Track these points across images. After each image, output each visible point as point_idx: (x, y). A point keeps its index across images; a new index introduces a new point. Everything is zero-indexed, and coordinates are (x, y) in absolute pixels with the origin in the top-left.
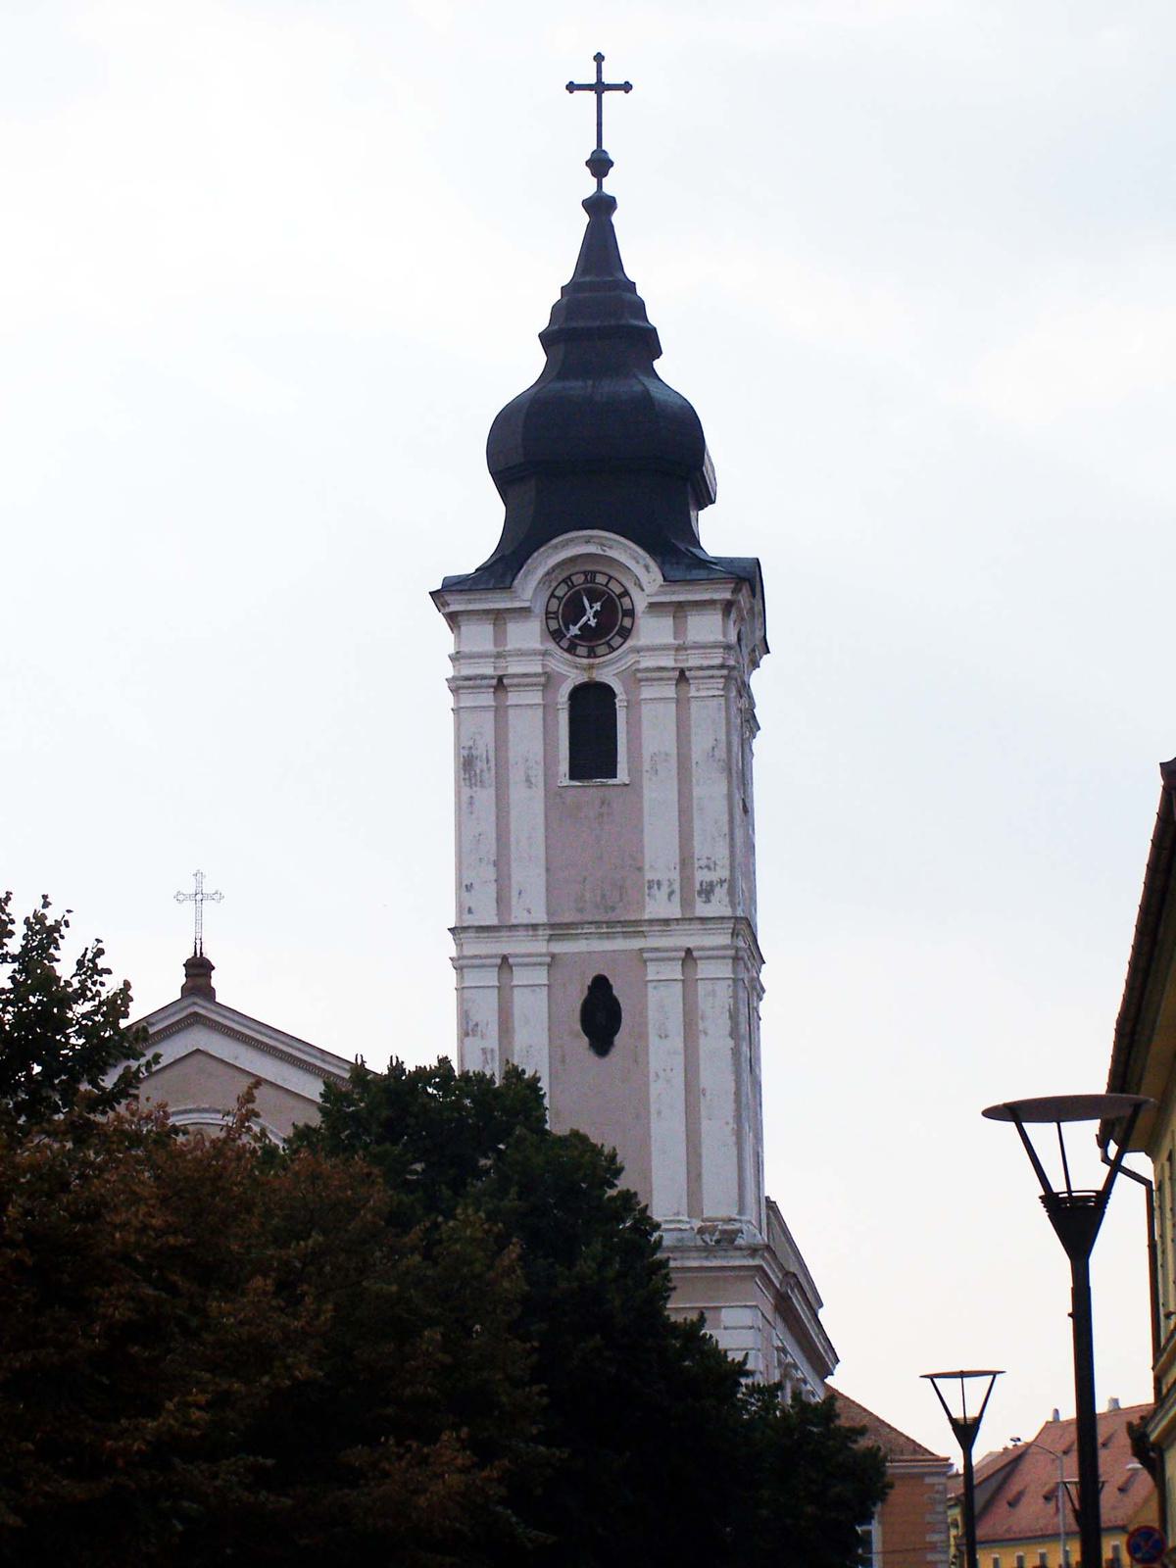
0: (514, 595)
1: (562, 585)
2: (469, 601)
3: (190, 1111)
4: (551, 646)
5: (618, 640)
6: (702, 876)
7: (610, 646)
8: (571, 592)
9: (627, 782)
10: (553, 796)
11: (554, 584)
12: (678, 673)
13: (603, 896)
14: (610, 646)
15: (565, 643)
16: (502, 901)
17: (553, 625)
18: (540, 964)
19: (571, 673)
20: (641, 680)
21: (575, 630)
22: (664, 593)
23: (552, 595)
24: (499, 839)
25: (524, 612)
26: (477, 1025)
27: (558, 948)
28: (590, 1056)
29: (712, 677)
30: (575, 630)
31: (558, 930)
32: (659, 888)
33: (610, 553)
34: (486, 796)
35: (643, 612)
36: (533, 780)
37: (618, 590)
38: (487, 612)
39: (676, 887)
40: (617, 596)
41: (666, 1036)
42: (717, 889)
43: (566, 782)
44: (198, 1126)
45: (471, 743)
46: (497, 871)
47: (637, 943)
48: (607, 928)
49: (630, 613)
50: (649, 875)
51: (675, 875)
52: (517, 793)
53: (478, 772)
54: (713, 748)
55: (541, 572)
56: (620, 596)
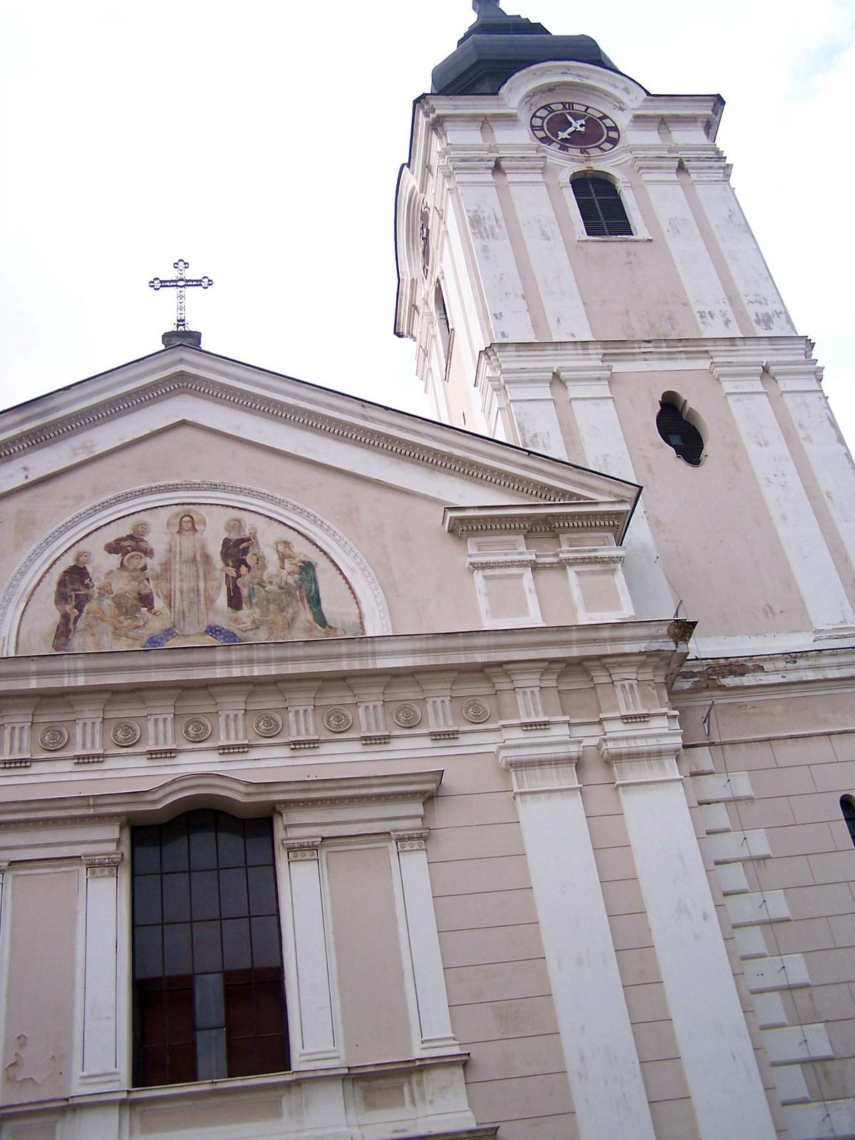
0: (501, 103)
1: (542, 110)
2: (456, 107)
3: (175, 488)
5: (607, 146)
8: (551, 115)
9: (651, 238)
10: (573, 249)
12: (677, 163)
13: (652, 326)
14: (601, 149)
16: (538, 320)
17: (541, 134)
18: (599, 379)
20: (640, 168)
21: (563, 135)
22: (647, 108)
23: (534, 116)
24: (523, 278)
25: (510, 119)
26: (535, 436)
28: (682, 464)
29: (710, 168)
31: (614, 348)
32: (712, 317)
34: (502, 248)
35: (628, 126)
36: (550, 234)
38: (474, 118)
39: (731, 316)
40: (598, 118)
41: (766, 445)
42: (775, 319)
44: (186, 507)
45: (476, 208)
46: (527, 304)
49: (615, 129)
50: (696, 309)
51: (727, 307)
52: (534, 246)
53: (488, 227)
54: (730, 217)
55: (524, 91)
56: (601, 118)
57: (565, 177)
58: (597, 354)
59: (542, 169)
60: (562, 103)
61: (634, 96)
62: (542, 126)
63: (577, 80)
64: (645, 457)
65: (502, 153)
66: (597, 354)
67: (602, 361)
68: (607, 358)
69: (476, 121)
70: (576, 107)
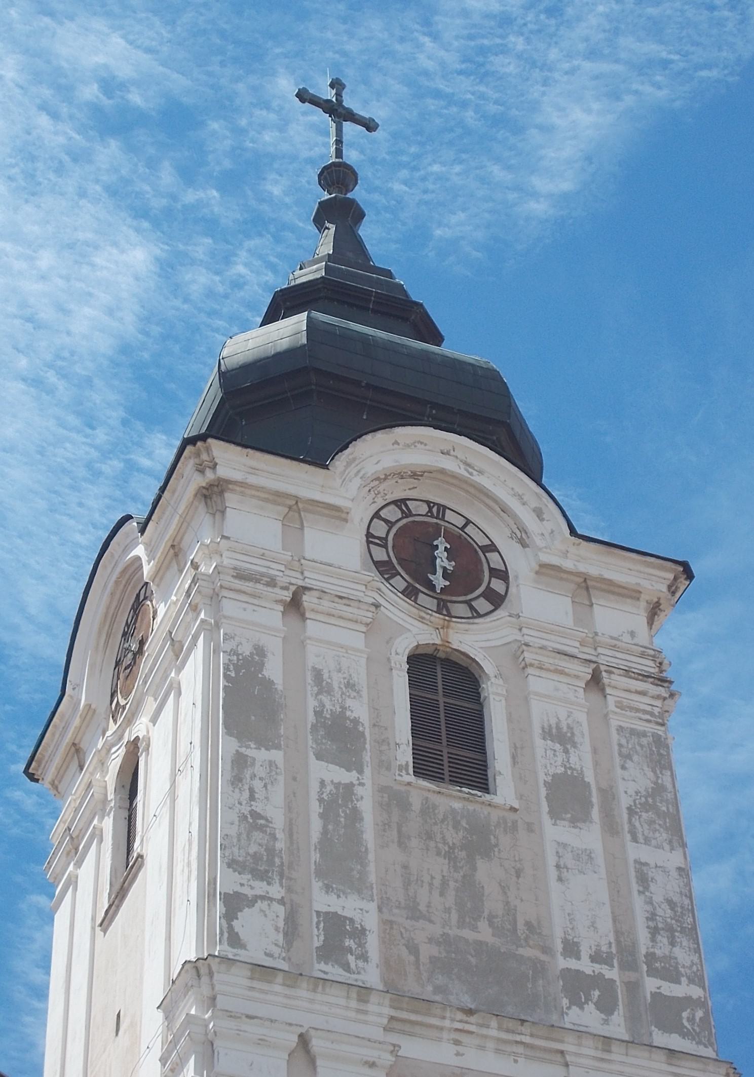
5: (482, 605)
7: (472, 608)
8: (405, 521)
11: (380, 502)
14: (472, 608)
17: (380, 554)
23: (377, 515)
33: (477, 478)
38: (277, 497)
48: (500, 1028)
49: (503, 575)
57: (403, 647)
58: (380, 1015)
59: (367, 625)
60: (428, 503)
61: (548, 526)
62: (386, 539)
63: (462, 471)
65: (313, 579)
66: (380, 1015)
67: (385, 1029)
68: (396, 1025)
69: (275, 503)
70: (449, 516)
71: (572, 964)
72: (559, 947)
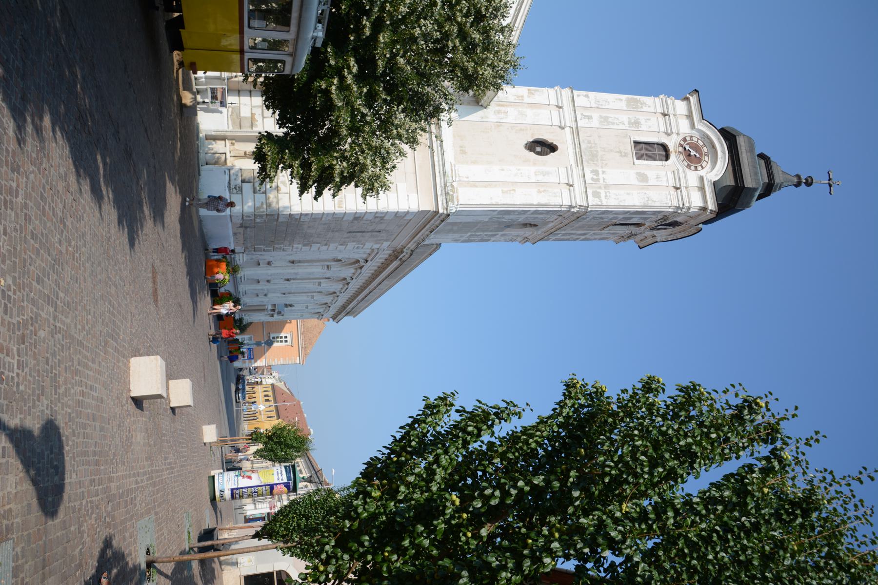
4: (681, 137)
6: (603, 193)
15: (682, 143)
17: (688, 138)
19: (672, 143)
22: (708, 181)
25: (693, 126)
27: (568, 130)
30: (687, 147)
31: (576, 131)
37: (704, 166)
43: (632, 140)
47: (572, 161)
64: (527, 130)
71: (600, 172)
72: (604, 170)
